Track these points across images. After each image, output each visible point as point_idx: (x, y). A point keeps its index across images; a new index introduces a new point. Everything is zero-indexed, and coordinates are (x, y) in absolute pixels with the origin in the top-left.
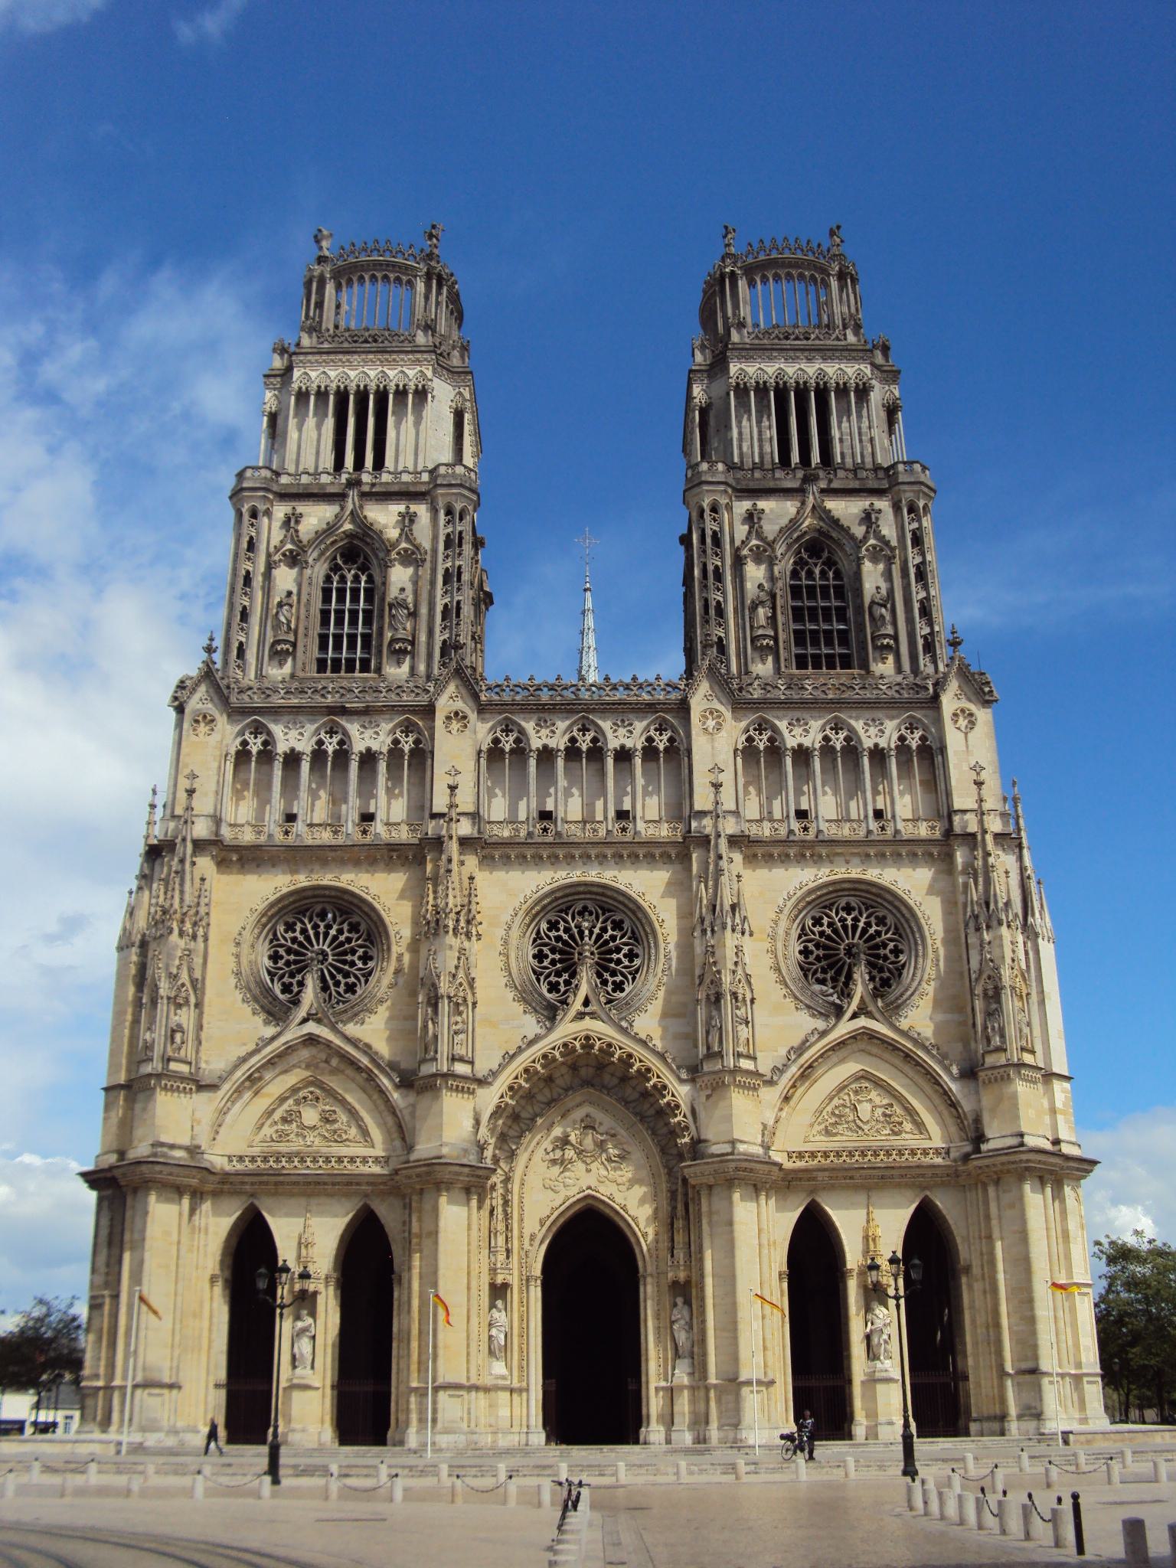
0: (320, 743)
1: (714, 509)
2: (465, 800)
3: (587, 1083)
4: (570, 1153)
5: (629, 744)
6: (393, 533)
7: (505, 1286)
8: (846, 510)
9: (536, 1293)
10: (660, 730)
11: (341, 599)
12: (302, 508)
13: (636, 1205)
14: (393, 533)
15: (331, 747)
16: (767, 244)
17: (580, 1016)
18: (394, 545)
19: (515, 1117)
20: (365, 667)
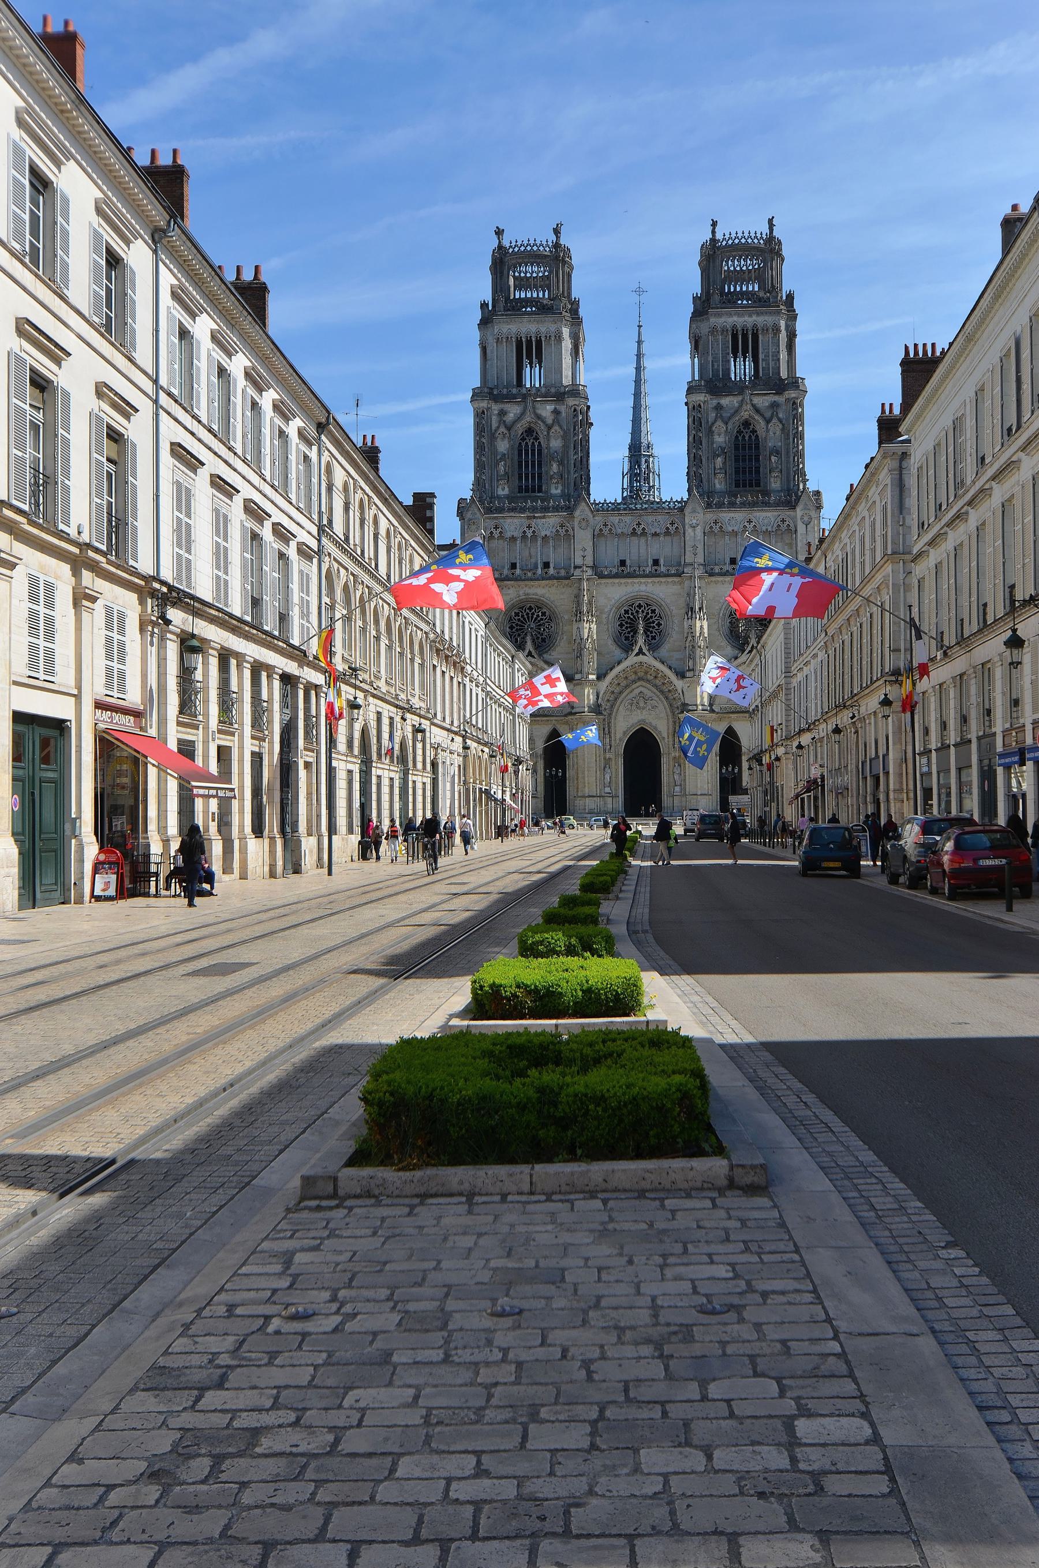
0: (524, 532)
1: (700, 406)
2: (589, 561)
3: (640, 679)
4: (634, 707)
5: (658, 531)
6: (550, 421)
7: (610, 759)
8: (763, 401)
9: (621, 761)
10: (672, 524)
11: (527, 454)
12: (507, 407)
13: (660, 725)
14: (550, 421)
15: (529, 534)
16: (733, 236)
17: (637, 654)
18: (549, 428)
19: (613, 692)
20: (540, 491)
